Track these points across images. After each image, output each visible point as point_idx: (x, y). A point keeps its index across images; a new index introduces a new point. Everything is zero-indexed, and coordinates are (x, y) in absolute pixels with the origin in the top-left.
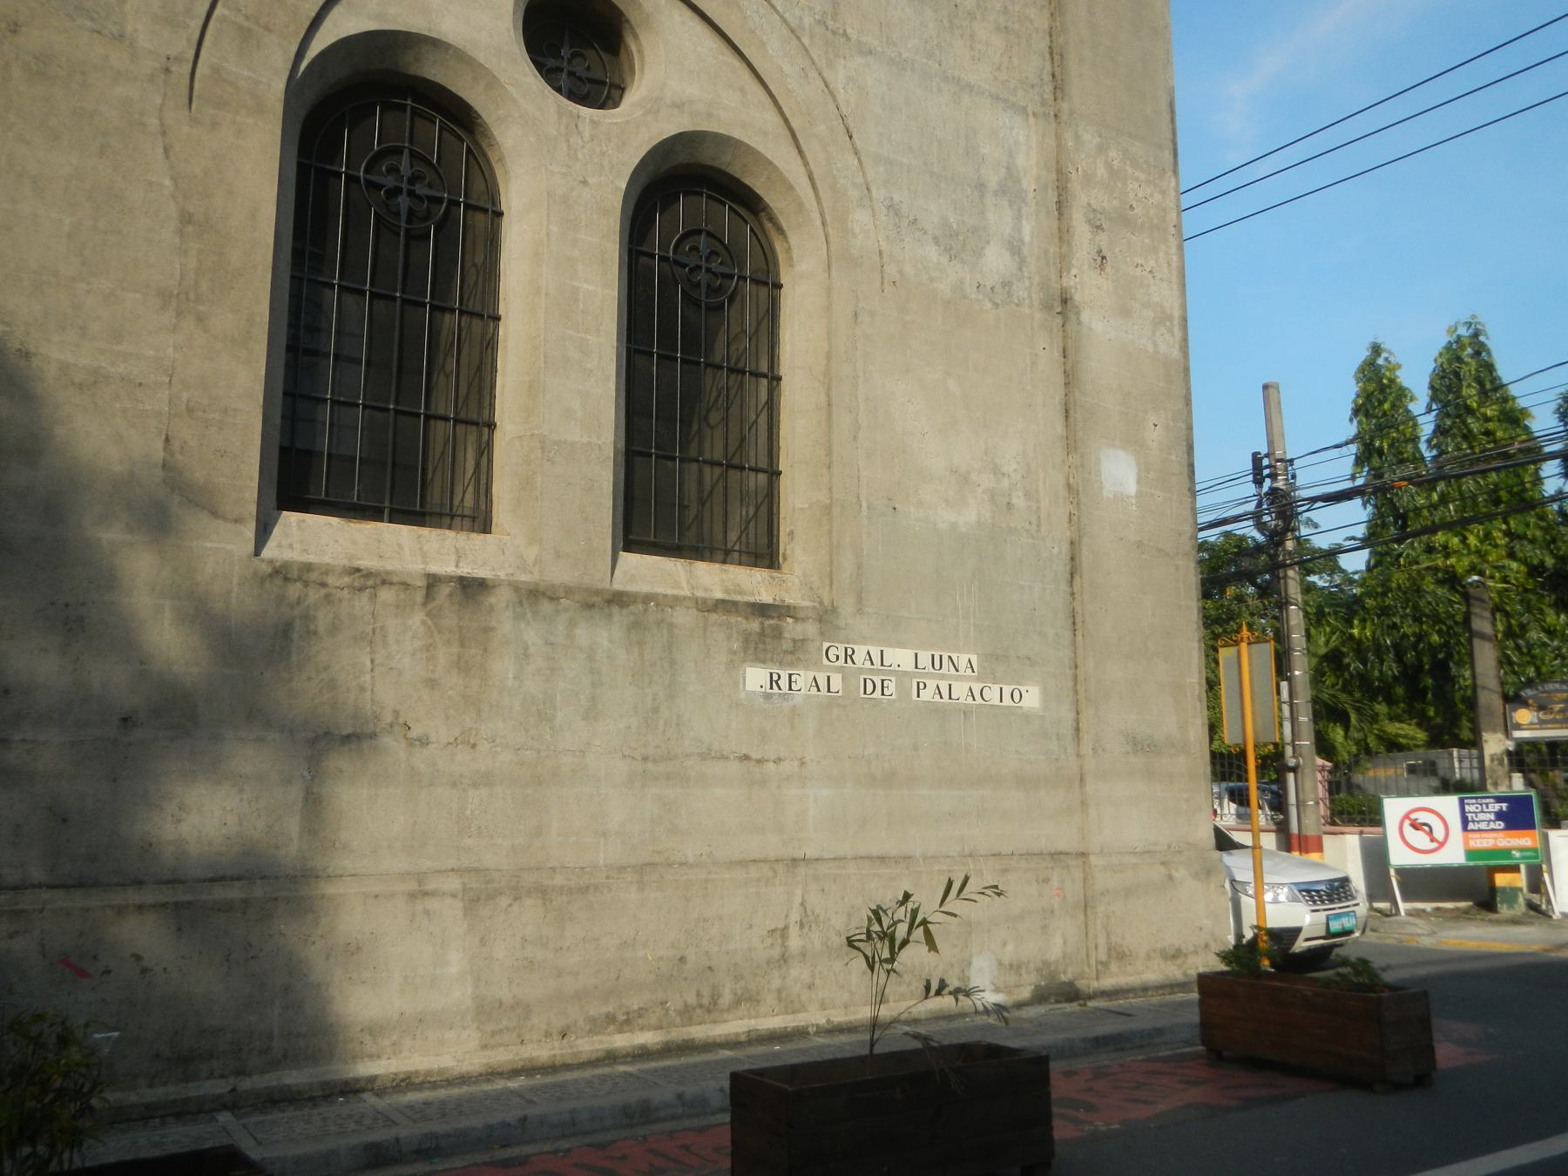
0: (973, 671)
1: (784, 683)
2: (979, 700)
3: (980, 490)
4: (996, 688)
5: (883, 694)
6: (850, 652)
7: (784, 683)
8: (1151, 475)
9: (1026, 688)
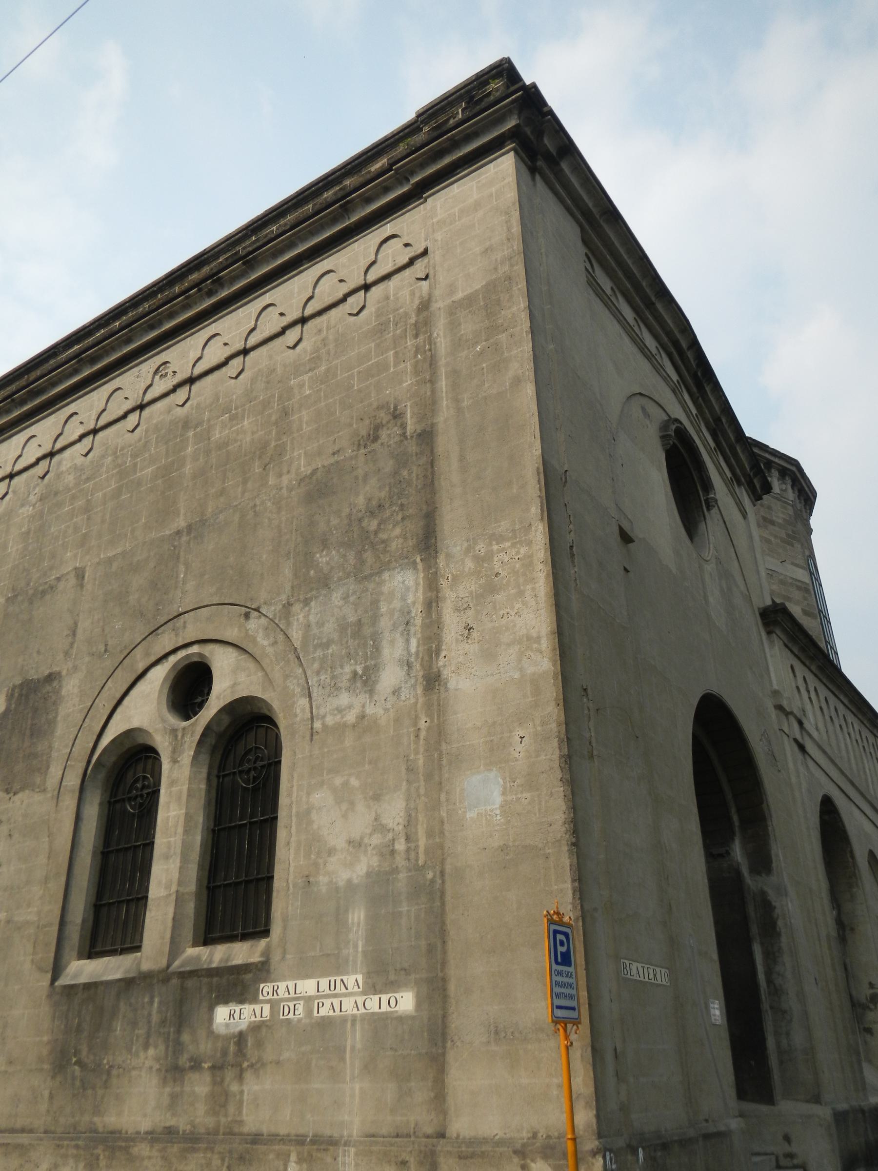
0: (359, 988)
1: (237, 1016)
2: (362, 1010)
3: (370, 849)
4: (376, 998)
5: (294, 1014)
6: (276, 988)
7: (237, 1016)
8: (518, 781)
9: (401, 994)
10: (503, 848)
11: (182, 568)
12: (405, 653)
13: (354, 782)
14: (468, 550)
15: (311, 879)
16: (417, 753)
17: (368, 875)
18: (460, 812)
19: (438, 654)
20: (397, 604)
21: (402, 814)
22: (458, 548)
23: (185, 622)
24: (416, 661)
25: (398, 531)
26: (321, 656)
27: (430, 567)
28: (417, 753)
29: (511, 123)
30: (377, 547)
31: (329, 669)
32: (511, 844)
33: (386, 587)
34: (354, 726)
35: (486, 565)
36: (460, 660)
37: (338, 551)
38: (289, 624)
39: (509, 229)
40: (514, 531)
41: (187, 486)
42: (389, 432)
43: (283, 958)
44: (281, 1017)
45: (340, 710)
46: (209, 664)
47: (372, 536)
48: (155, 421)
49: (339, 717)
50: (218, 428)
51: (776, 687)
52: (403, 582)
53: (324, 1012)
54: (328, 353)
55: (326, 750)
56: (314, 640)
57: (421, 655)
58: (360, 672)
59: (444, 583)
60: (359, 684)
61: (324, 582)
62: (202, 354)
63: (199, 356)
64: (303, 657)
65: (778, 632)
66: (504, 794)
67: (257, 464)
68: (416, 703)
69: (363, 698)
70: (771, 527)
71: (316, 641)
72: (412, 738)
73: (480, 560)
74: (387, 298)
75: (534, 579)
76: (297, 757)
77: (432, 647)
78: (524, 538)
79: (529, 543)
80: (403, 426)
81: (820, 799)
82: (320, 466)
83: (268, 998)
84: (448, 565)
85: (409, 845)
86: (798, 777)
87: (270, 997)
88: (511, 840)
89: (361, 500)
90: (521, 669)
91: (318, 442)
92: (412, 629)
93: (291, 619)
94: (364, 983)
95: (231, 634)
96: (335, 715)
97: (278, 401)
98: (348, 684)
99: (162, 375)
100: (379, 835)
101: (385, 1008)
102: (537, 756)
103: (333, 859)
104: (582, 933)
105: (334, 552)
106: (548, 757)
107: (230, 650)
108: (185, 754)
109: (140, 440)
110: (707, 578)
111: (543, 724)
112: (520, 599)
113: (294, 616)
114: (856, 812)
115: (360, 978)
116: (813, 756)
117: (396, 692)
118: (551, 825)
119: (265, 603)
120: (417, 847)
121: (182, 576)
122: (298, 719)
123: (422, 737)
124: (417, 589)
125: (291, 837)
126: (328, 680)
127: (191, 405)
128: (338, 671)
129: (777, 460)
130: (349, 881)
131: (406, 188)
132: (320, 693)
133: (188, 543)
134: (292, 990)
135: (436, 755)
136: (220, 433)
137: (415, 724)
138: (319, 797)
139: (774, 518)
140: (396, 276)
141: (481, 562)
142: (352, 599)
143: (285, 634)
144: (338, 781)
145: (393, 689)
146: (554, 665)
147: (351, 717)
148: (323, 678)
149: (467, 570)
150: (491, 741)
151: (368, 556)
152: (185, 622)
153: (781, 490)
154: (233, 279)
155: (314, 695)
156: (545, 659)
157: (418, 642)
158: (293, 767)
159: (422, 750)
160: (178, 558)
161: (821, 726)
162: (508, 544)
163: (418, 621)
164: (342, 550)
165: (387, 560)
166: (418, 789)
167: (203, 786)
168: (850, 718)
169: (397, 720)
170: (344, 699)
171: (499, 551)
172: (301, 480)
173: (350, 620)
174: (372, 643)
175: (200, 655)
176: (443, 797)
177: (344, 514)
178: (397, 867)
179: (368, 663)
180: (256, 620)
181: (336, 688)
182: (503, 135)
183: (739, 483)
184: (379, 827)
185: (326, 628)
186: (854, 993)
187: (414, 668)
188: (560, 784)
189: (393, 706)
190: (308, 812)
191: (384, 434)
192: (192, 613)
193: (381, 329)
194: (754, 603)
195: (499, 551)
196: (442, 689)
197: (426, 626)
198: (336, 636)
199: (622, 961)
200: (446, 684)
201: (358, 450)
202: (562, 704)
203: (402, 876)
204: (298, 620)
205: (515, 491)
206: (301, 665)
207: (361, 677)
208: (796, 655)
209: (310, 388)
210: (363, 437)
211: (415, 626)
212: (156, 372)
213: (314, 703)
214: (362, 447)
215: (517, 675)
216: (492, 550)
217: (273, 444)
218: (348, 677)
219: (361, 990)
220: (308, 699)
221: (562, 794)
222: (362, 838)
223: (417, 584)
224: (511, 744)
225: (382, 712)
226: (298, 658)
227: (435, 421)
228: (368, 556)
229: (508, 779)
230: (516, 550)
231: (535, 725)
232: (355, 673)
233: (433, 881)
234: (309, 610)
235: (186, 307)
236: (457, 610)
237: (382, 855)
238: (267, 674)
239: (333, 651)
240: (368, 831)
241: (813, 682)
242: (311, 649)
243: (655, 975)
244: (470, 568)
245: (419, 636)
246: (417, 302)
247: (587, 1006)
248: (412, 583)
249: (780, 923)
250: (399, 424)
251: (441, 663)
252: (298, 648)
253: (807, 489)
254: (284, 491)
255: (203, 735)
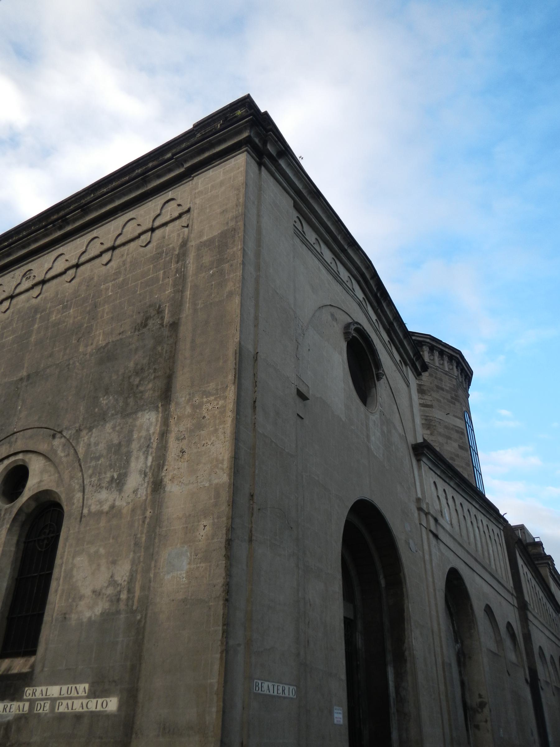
3: (105, 597)
4: (94, 701)
5: (43, 710)
6: (35, 691)
7: (8, 710)
8: (199, 555)
9: (111, 699)
10: (185, 601)
11: (20, 403)
12: (144, 466)
13: (102, 551)
14: (189, 401)
15: (67, 616)
16: (142, 533)
17: (102, 614)
18: (162, 574)
19: (163, 468)
20: (144, 433)
21: (128, 574)
22: (183, 399)
23: (17, 438)
24: (150, 471)
25: (150, 386)
26: (94, 465)
27: (166, 410)
28: (142, 533)
29: (245, 135)
30: (137, 395)
31: (98, 474)
32: (189, 598)
33: (139, 422)
34: (107, 513)
35: (198, 411)
36: (175, 472)
37: (114, 397)
38: (78, 443)
39: (238, 199)
40: (217, 390)
41: (31, 350)
42: (153, 322)
43: (42, 670)
44: (35, 712)
45: (101, 503)
46: (28, 467)
47: (135, 388)
48: (18, 307)
49: (99, 506)
50: (55, 313)
51: (420, 495)
52: (149, 419)
53: (62, 709)
54: (125, 270)
55: (88, 528)
56: (91, 454)
57: (153, 468)
58: (116, 477)
59: (172, 421)
60: (114, 485)
61: (103, 417)
62: (52, 266)
63: (50, 267)
64: (83, 465)
65: (424, 459)
66: (189, 563)
67: (74, 337)
68: (146, 500)
69: (115, 495)
70: (441, 391)
71: (92, 455)
72: (141, 522)
73: (194, 407)
74: (164, 238)
75: (225, 421)
76: (70, 532)
77: (160, 463)
78: (222, 395)
79: (225, 398)
80: (162, 318)
81: (447, 570)
82: (111, 341)
83: (29, 698)
84: (176, 409)
85: (129, 595)
86: (430, 555)
87: (30, 697)
88: (190, 595)
89: (131, 364)
90: (210, 481)
91: (112, 325)
92: (150, 450)
93: (80, 440)
94: (90, 690)
95: (43, 447)
96: (97, 505)
97: (92, 298)
98: (107, 485)
99: (27, 278)
100: (112, 588)
101: (99, 708)
102: (213, 539)
103: (82, 603)
104: (224, 662)
105: (111, 398)
106: (218, 540)
107: (41, 458)
108: (4, 527)
109: (8, 318)
110: (371, 424)
111: (218, 517)
112: (215, 435)
113: (82, 438)
114: (478, 579)
115: (87, 686)
116: (445, 542)
117: (135, 491)
118: (215, 586)
119: (66, 428)
120: (134, 597)
121: (20, 408)
122: (74, 507)
123: (146, 523)
124: (157, 424)
125: (59, 586)
126: (96, 482)
127: (42, 298)
128: (103, 476)
129: (447, 350)
130: (90, 618)
131: (182, 170)
132: (90, 490)
133: (26, 386)
134: (44, 693)
135: (153, 535)
136: (56, 316)
137: (144, 513)
138: (81, 561)
139: (444, 387)
140: (170, 224)
141: (195, 409)
142: (117, 428)
143: (75, 450)
144: (92, 550)
145: (133, 490)
146: (230, 479)
147: (106, 508)
148: (93, 479)
149: (186, 413)
150: (187, 527)
151: (131, 401)
152: (17, 438)
153: (449, 369)
154: (75, 220)
155: (86, 491)
156: (225, 475)
157: (153, 459)
158: (67, 539)
159: (145, 531)
160: (19, 396)
161: (455, 522)
162: (213, 398)
163: (155, 445)
164: (116, 396)
165: (142, 404)
166: (139, 557)
167: (13, 549)
168: (480, 517)
169: (133, 510)
170: (104, 495)
171: (207, 402)
172: (98, 349)
173: (114, 443)
174: (125, 458)
175: (23, 460)
176: (153, 565)
177: (120, 373)
178: (120, 610)
179: (121, 472)
180: (59, 440)
181: (101, 488)
182: (240, 141)
183: (406, 364)
184: (112, 582)
185: (99, 447)
186: (468, 701)
187: (148, 476)
188: (224, 558)
189: (132, 500)
190: (72, 570)
191: (150, 322)
192: (21, 433)
193: (158, 256)
194: (408, 440)
195: (207, 402)
196: (162, 491)
197: (158, 448)
198: (104, 452)
199: (255, 681)
200: (164, 488)
201: (135, 332)
202: (231, 505)
203: (122, 616)
204: (84, 440)
205: (221, 364)
206: (82, 471)
207: (116, 480)
208: (438, 475)
209: (112, 291)
210: (138, 324)
211: (152, 448)
212: (24, 276)
213: (85, 497)
214: (137, 331)
215: (207, 485)
216: (203, 401)
217: (85, 325)
218: (108, 480)
219: (86, 694)
220: (82, 494)
221: (224, 565)
222: (101, 590)
223: (157, 421)
224: (198, 530)
225: (125, 504)
226: (80, 466)
227: (181, 316)
228: (131, 401)
229: (193, 553)
230: (217, 402)
231: (213, 518)
232: (113, 477)
233: (140, 621)
234: (91, 435)
235: (45, 236)
236: (178, 439)
237: (111, 601)
238: (60, 476)
239: (102, 462)
240: (106, 585)
241: (450, 492)
242: (89, 460)
243: (283, 691)
244: (188, 412)
245: (154, 455)
246: (180, 241)
247: (221, 713)
248: (154, 420)
249: (407, 653)
250: (160, 317)
251: (163, 474)
252: (81, 459)
253: (466, 369)
254: (88, 356)
255: (17, 514)
